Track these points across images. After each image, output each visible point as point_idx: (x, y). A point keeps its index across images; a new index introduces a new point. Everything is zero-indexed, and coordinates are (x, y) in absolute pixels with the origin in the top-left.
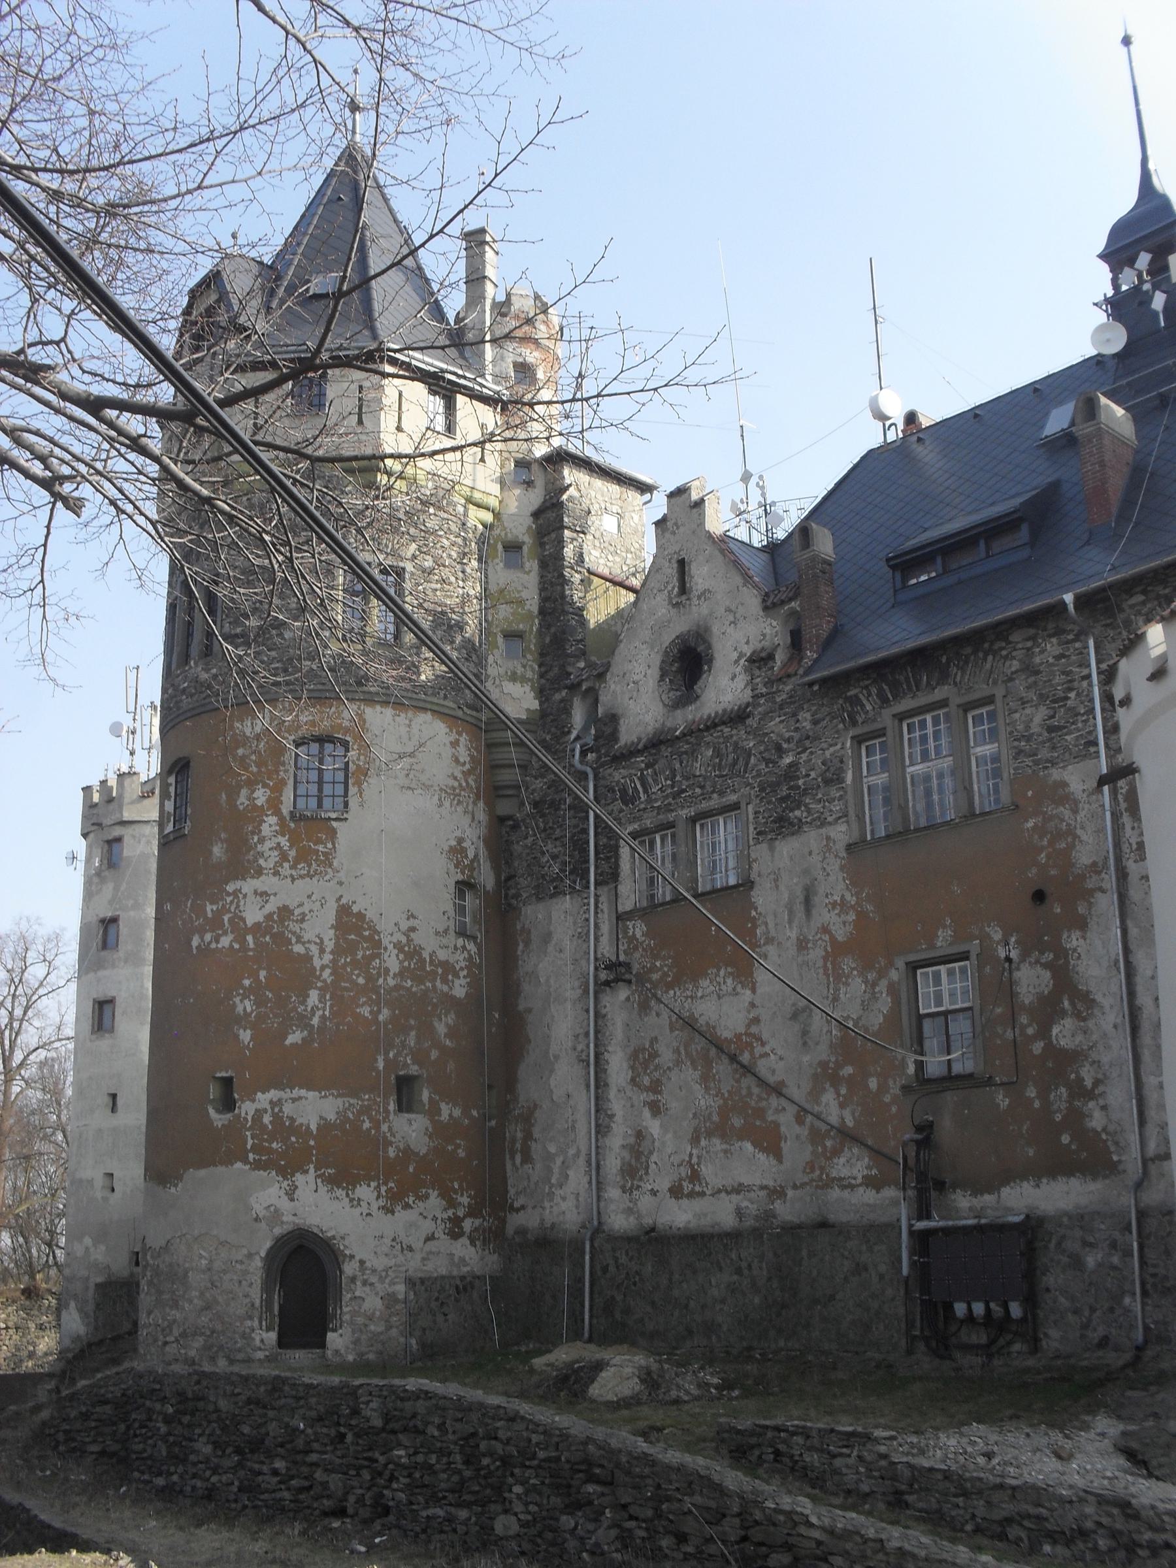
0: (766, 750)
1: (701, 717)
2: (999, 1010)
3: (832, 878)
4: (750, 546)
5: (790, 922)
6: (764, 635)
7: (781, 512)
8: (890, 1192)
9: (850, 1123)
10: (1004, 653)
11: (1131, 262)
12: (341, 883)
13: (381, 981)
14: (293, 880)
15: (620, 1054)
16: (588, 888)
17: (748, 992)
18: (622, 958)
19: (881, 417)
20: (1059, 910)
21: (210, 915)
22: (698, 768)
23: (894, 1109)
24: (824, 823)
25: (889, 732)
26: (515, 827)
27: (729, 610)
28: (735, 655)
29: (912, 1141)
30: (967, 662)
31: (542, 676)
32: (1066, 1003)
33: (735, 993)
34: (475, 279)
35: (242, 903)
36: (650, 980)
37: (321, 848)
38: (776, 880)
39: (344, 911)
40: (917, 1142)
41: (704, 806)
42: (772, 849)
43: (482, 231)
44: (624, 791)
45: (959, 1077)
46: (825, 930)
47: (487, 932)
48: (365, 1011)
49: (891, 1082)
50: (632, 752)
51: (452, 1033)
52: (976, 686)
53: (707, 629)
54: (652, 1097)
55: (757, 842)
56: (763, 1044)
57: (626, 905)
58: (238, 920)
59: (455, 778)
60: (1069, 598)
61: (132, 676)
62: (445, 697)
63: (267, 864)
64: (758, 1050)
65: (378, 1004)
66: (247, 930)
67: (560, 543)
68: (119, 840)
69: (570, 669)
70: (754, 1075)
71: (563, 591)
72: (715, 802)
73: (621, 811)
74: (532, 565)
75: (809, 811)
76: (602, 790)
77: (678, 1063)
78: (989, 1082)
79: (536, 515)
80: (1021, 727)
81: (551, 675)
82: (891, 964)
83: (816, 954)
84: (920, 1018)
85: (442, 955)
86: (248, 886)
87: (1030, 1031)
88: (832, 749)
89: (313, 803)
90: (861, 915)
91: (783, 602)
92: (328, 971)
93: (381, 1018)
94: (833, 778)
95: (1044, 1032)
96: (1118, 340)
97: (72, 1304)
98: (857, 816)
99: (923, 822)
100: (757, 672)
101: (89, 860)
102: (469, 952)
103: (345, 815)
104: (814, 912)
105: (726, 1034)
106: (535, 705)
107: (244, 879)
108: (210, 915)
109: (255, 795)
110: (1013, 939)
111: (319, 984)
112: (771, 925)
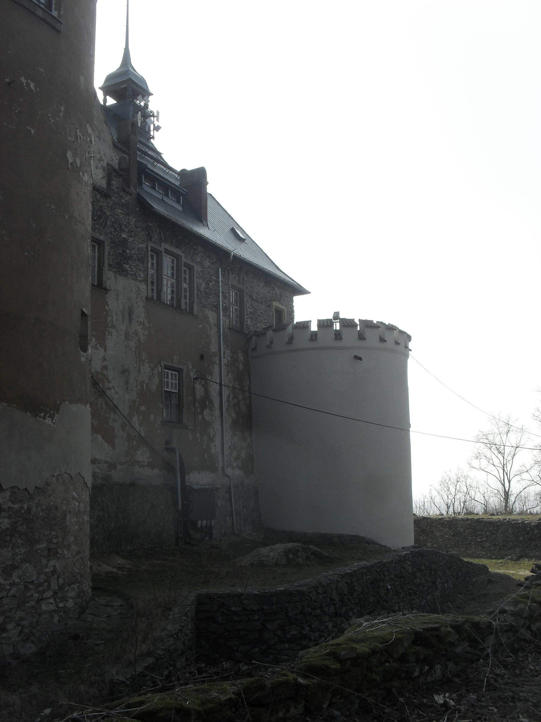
8: (156, 471)
17: (103, 350)
46: (136, 333)
83: (132, 344)
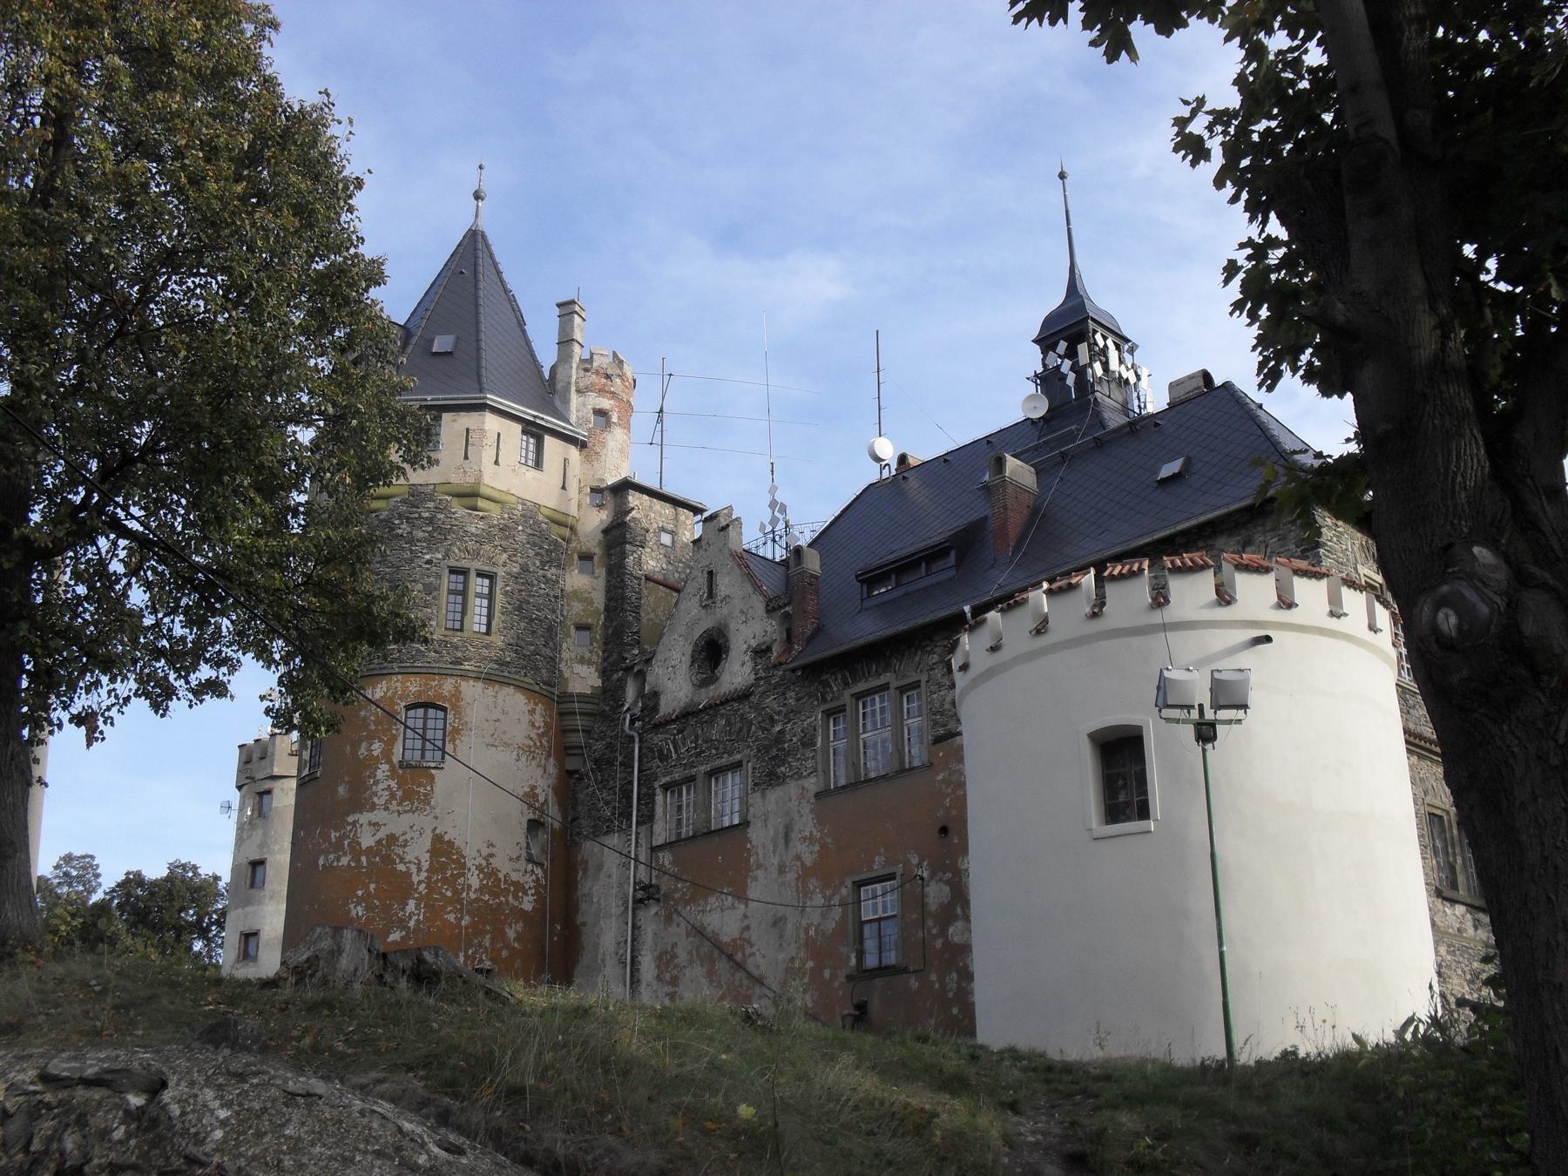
0: (763, 721)
1: (719, 696)
2: (914, 916)
3: (804, 818)
4: (772, 561)
5: (774, 852)
6: (766, 632)
7: (797, 534)
9: (810, 1005)
10: (929, 648)
11: (1053, 347)
12: (436, 818)
13: (465, 894)
14: (399, 814)
15: (650, 956)
16: (631, 827)
17: (743, 906)
18: (654, 882)
19: (878, 459)
20: (956, 841)
21: (334, 840)
22: (714, 734)
23: (840, 993)
24: (800, 776)
25: (848, 709)
26: (580, 779)
27: (742, 612)
28: (745, 646)
29: (850, 1015)
30: (903, 657)
31: (605, 660)
32: (959, 910)
33: (733, 907)
34: (566, 342)
35: (359, 830)
36: (673, 899)
37: (422, 790)
38: (765, 821)
39: (437, 839)
40: (855, 1016)
41: (717, 763)
42: (763, 796)
43: (573, 302)
44: (660, 751)
45: (888, 967)
46: (798, 858)
47: (552, 860)
48: (451, 918)
49: (839, 972)
50: (668, 722)
51: (518, 938)
52: (909, 674)
53: (726, 626)
54: (672, 990)
55: (754, 791)
56: (752, 946)
57: (659, 840)
58: (355, 844)
59: (531, 739)
60: (967, 609)
62: (525, 675)
63: (379, 801)
64: (748, 950)
65: (462, 913)
66: (362, 852)
67: (623, 555)
68: (269, 792)
69: (626, 655)
70: (744, 969)
71: (623, 594)
72: (725, 760)
73: (659, 767)
74: (601, 572)
75: (791, 770)
76: (644, 751)
77: (691, 962)
78: (905, 970)
79: (606, 532)
80: (938, 705)
81: (611, 659)
82: (842, 883)
83: (791, 876)
84: (862, 923)
85: (515, 877)
86: (364, 818)
87: (934, 931)
88: (809, 720)
89: (418, 754)
90: (823, 847)
91: (780, 607)
92: (423, 885)
93: (463, 923)
94: (808, 742)
95: (943, 932)
96: (1041, 409)
98: (824, 771)
99: (873, 775)
100: (759, 661)
101: (241, 810)
102: (536, 875)
103: (442, 765)
104: (791, 844)
105: (726, 939)
106: (599, 683)
107: (361, 813)
108: (334, 840)
109: (373, 748)
110: (926, 863)
111: (416, 895)
112: (760, 856)
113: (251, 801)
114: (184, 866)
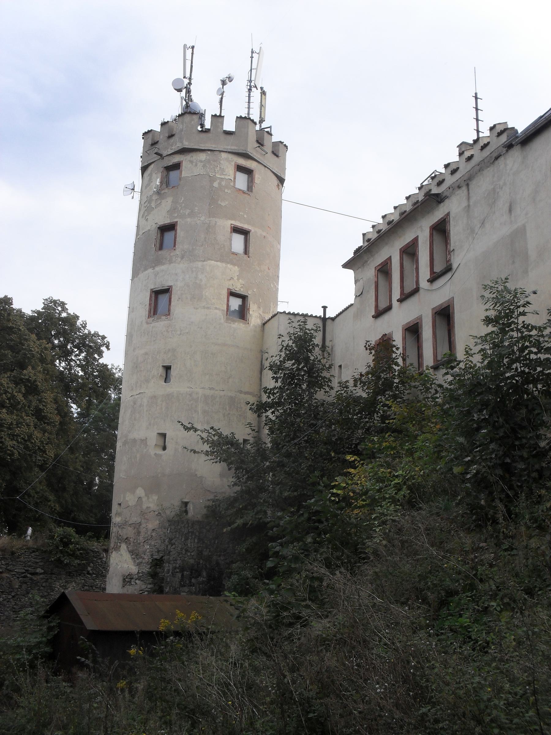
61: (189, 52)
68: (177, 166)
97: (124, 546)
113: (160, 175)
114: (55, 302)
